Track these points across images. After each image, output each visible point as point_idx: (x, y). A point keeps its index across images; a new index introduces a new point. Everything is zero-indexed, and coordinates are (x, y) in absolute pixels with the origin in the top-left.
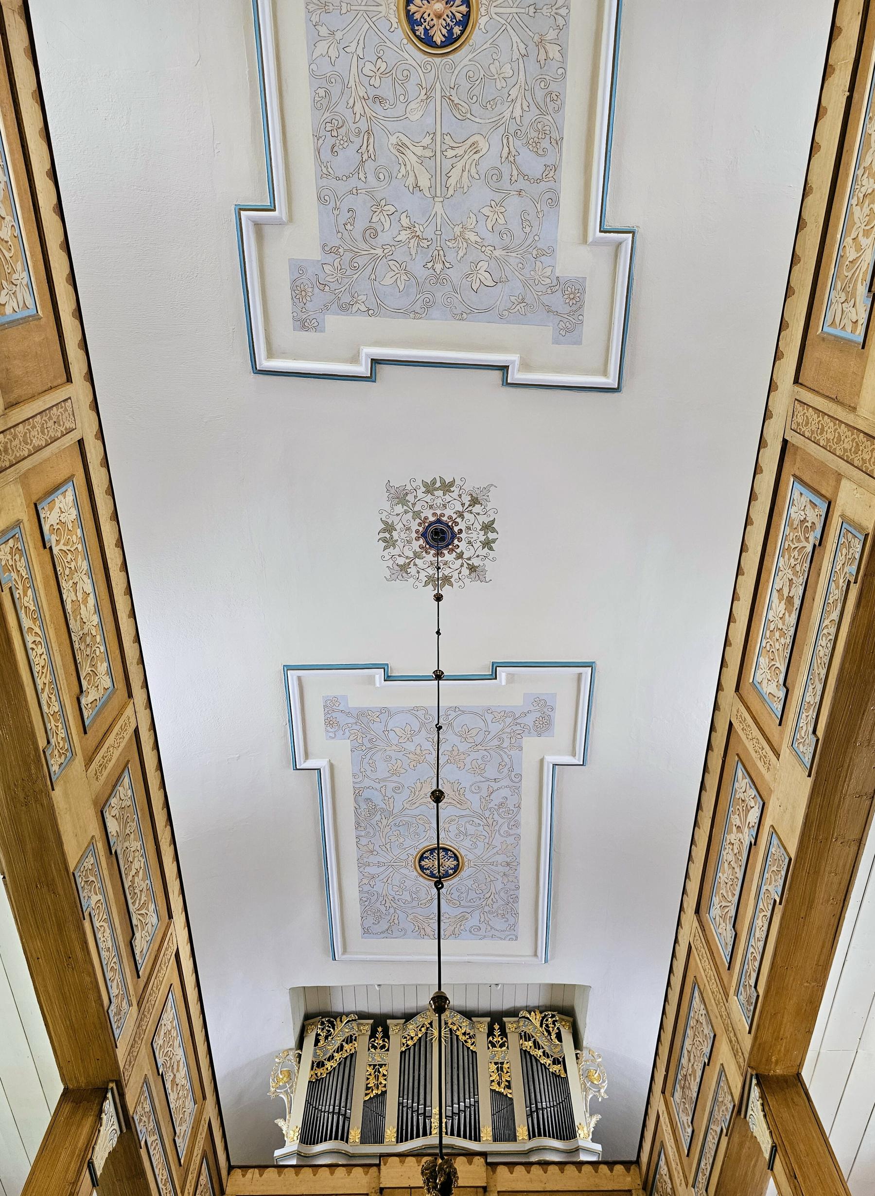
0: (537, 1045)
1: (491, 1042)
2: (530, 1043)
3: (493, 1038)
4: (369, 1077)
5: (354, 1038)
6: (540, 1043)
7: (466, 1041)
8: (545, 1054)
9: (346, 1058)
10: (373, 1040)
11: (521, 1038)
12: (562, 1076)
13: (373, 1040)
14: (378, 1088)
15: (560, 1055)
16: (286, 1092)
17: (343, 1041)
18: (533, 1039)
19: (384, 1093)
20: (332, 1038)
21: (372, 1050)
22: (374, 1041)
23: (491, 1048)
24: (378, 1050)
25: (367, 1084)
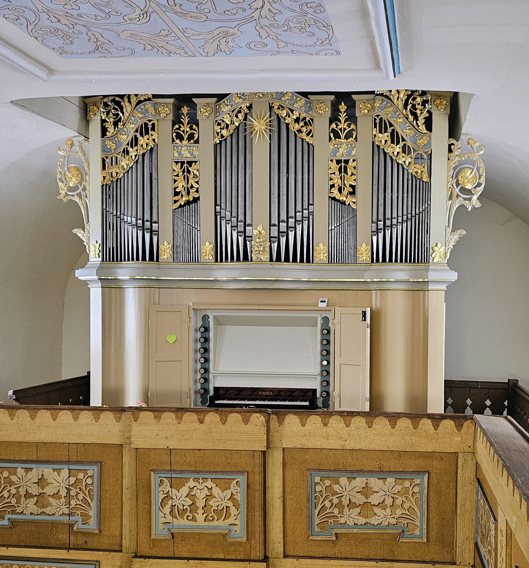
0: (395, 138)
1: (333, 131)
2: (386, 136)
3: (337, 125)
4: (176, 178)
5: (150, 126)
6: (400, 133)
7: (299, 131)
8: (404, 149)
9: (144, 155)
10: (177, 126)
11: (375, 127)
12: (424, 180)
13: (177, 126)
14: (188, 193)
15: (426, 150)
16: (79, 195)
17: (137, 131)
18: (390, 130)
19: (196, 200)
20: (123, 125)
21: (178, 141)
22: (179, 129)
23: (333, 138)
24: (185, 142)
25: (175, 188)
